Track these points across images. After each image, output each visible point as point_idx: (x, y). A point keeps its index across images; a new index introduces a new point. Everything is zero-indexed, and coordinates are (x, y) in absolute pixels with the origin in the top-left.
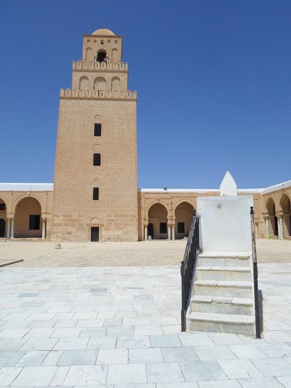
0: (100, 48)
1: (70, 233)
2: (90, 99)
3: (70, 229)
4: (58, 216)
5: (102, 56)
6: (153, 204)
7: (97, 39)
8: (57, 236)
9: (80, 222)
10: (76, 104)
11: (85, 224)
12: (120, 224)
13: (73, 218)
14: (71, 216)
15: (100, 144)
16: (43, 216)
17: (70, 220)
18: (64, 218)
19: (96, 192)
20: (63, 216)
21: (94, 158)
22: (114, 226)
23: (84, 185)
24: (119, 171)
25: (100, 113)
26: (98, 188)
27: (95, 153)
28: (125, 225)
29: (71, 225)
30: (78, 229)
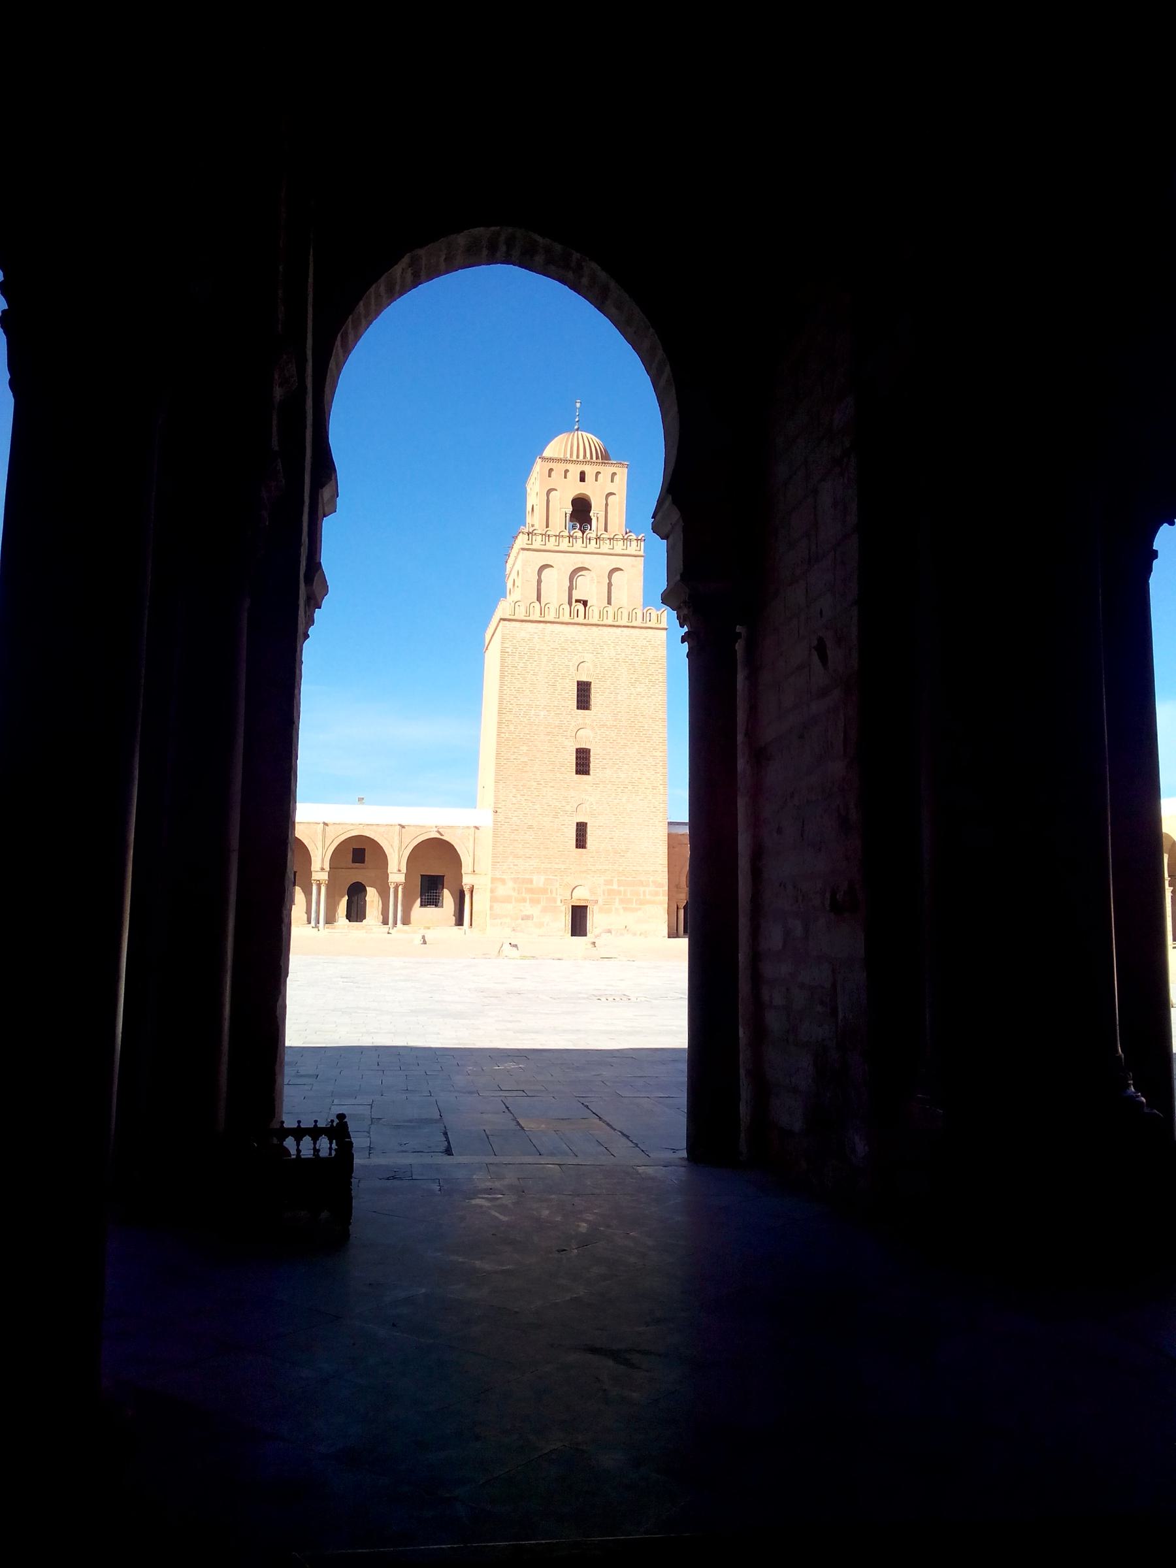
4: (503, 881)
5: (581, 511)
14: (531, 881)
15: (587, 728)
16: (467, 880)
19: (581, 829)
20: (515, 880)
23: (556, 817)
24: (630, 788)
25: (588, 657)
29: (532, 901)
30: (544, 910)
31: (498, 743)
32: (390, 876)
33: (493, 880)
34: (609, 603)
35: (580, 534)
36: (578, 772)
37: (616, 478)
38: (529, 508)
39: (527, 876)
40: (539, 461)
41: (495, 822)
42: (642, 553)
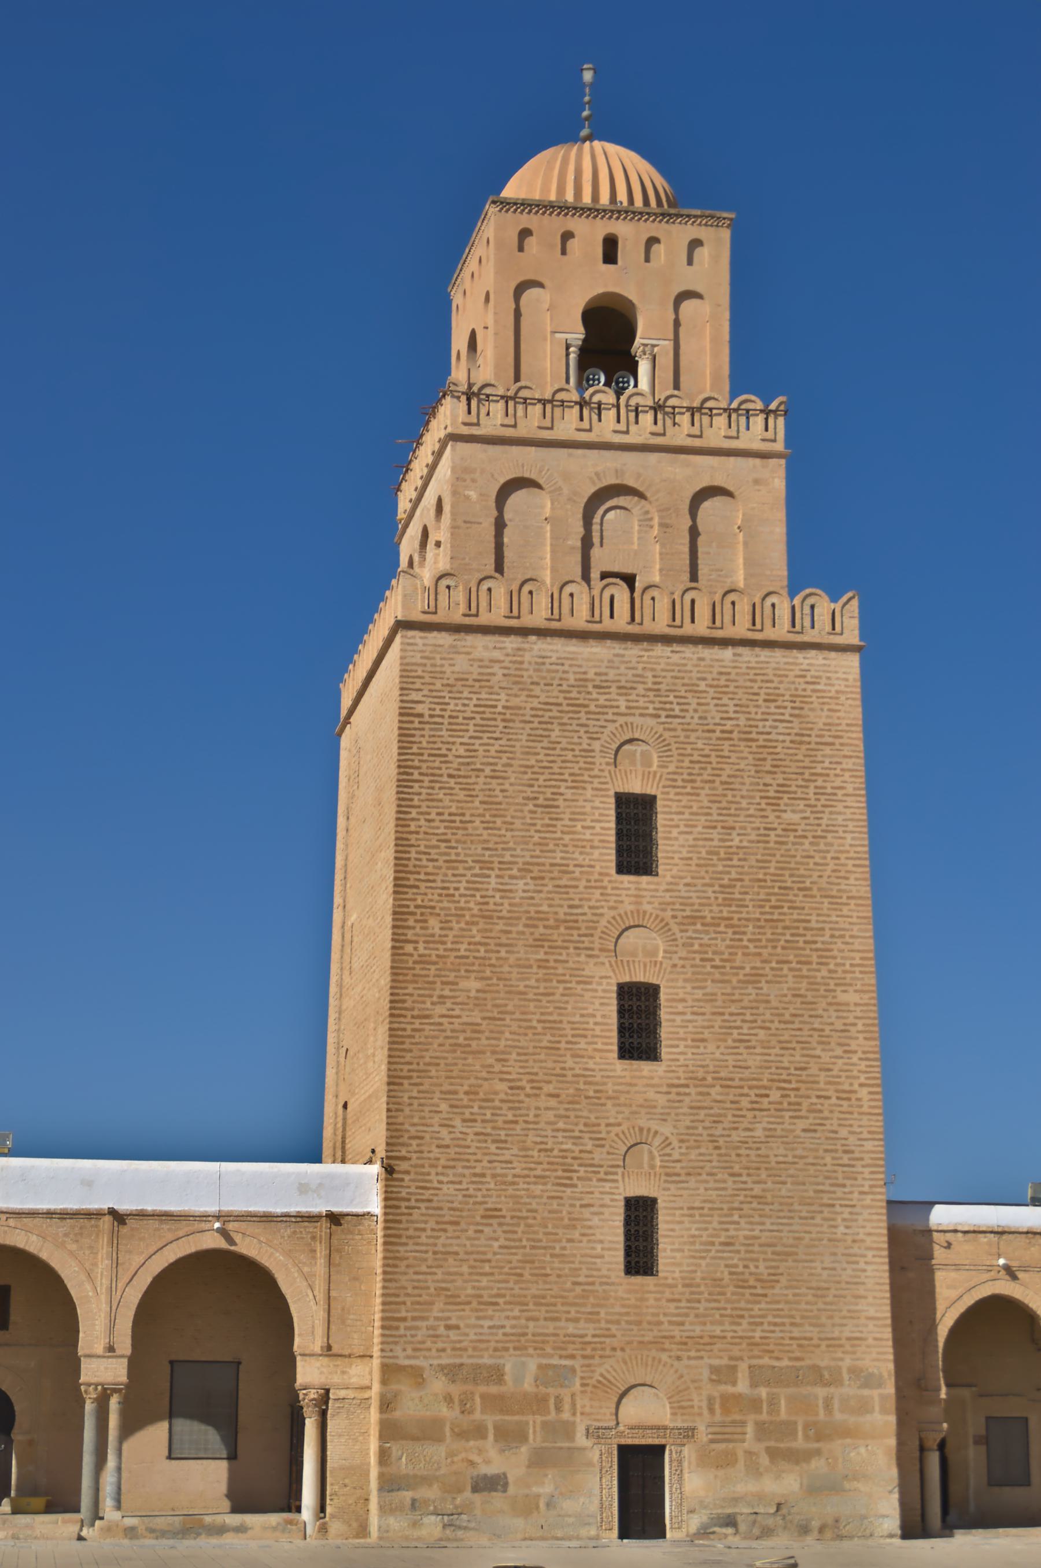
0: (601, 290)
1: (490, 1484)
2: (583, 636)
3: (493, 1460)
4: (417, 1376)
5: (607, 342)
6: (969, 1301)
7: (578, 225)
8: (414, 1501)
9: (553, 1415)
10: (496, 669)
11: (580, 1430)
12: (788, 1429)
13: (509, 1385)
14: (497, 1375)
16: (309, 1374)
17: (496, 1403)
18: (456, 1390)
20: (452, 1372)
21: (621, 1012)
22: (759, 1440)
24: (775, 1095)
25: (645, 726)
26: (654, 1201)
27: (627, 979)
28: (821, 1433)
30: (540, 1461)
31: (397, 971)
32: (84, 1365)
33: (389, 1371)
34: (694, 577)
35: (608, 397)
36: (626, 1052)
37: (703, 254)
38: (459, 342)
39: (486, 1360)
40: (491, 210)
41: (390, 1199)
42: (779, 446)
